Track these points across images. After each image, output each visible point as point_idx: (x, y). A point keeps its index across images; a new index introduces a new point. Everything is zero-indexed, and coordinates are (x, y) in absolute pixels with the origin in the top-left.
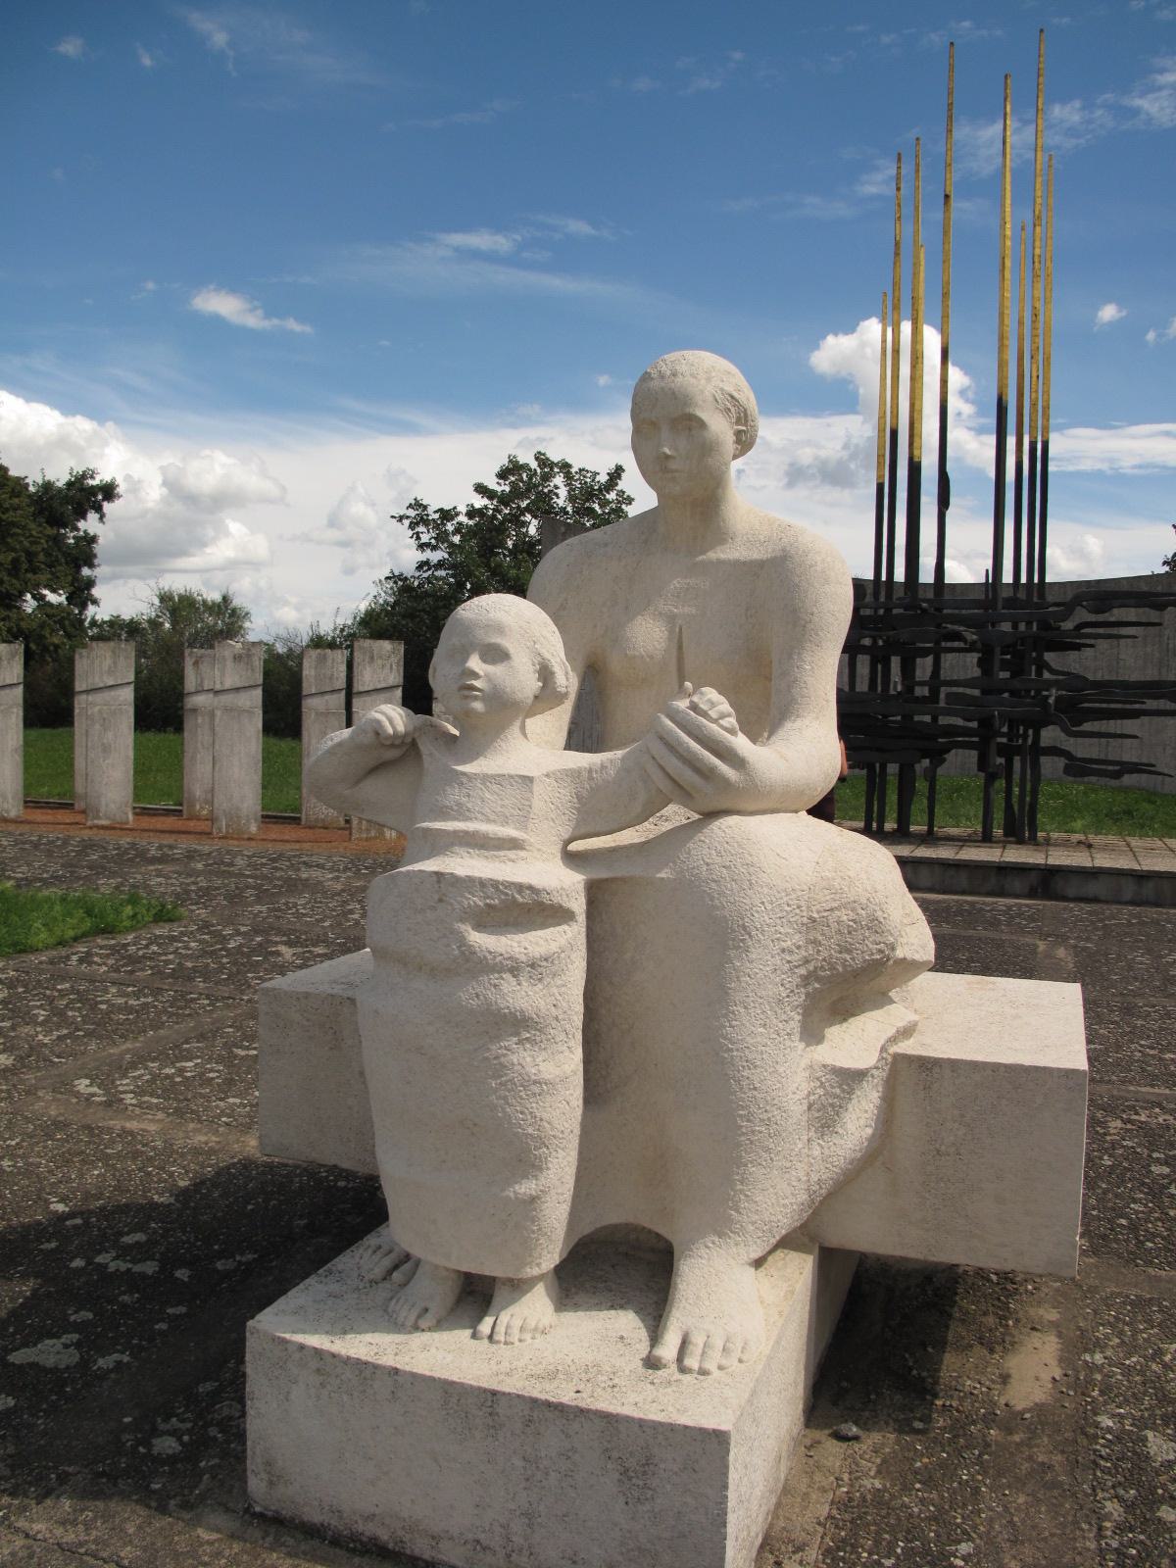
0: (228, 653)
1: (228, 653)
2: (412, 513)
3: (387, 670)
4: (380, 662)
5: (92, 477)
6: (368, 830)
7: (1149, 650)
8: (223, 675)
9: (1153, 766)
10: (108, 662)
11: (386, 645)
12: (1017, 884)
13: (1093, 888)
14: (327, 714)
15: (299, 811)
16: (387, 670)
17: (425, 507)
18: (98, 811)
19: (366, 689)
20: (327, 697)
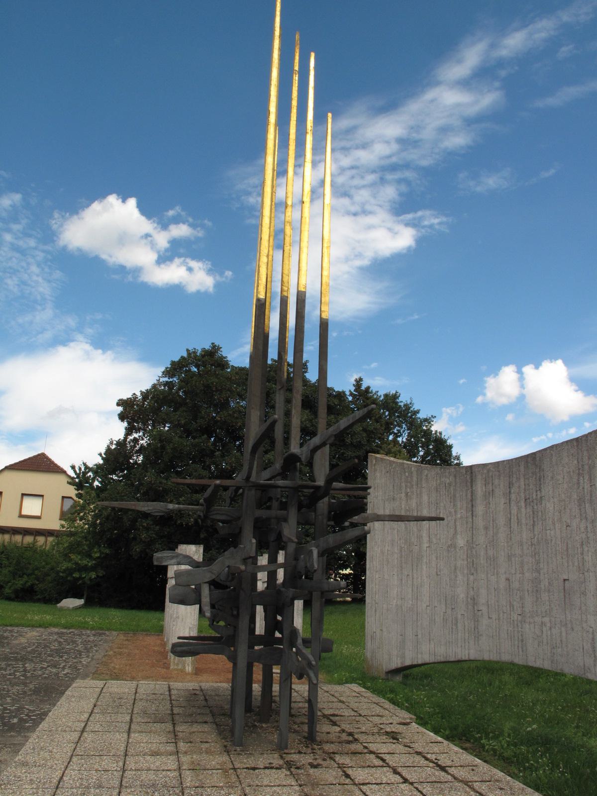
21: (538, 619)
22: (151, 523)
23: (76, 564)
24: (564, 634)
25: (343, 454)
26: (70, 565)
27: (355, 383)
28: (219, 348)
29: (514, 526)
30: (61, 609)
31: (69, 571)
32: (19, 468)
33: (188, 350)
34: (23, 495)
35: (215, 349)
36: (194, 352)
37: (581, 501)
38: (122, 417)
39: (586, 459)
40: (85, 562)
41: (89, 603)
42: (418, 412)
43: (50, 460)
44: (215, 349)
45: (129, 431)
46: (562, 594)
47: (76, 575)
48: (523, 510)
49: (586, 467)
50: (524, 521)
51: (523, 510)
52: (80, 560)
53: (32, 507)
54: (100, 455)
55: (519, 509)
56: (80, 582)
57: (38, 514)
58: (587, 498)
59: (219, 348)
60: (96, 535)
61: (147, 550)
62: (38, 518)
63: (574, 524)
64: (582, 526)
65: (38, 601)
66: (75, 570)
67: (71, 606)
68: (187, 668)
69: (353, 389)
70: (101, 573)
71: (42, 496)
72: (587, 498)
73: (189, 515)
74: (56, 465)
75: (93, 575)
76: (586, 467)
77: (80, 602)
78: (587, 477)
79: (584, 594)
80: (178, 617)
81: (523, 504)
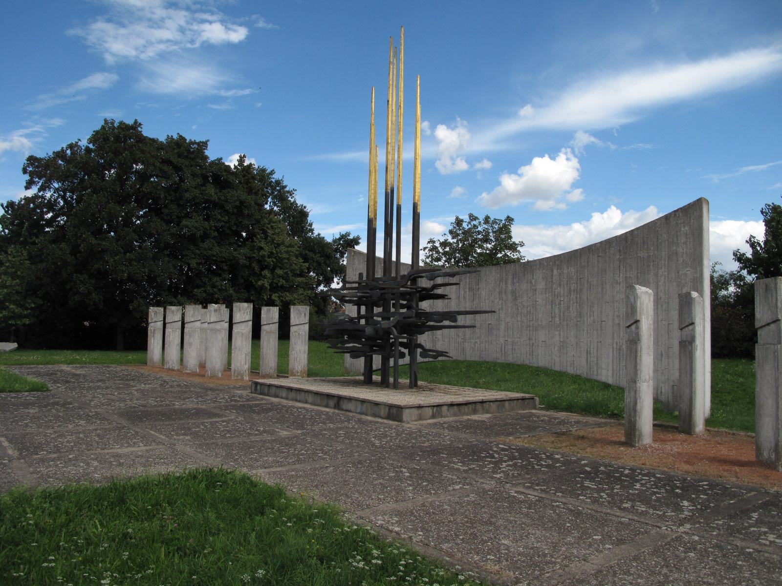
0: (212, 309)
1: (212, 309)
2: (429, 245)
3: (245, 314)
4: (243, 311)
5: (349, 236)
6: (237, 376)
7: (547, 295)
8: (210, 316)
9: (447, 353)
10: (192, 312)
11: (246, 305)
12: (332, 403)
13: (351, 406)
14: (271, 332)
15: (258, 369)
16: (245, 314)
17: (434, 242)
18: (187, 367)
19: (238, 321)
20: (271, 325)
21: (473, 341)
23: (13, 312)
24: (487, 346)
25: (241, 222)
27: (239, 158)
29: (462, 299)
35: (137, 124)
36: (113, 123)
37: (500, 293)
39: (504, 275)
40: (18, 310)
41: (22, 347)
42: (285, 187)
44: (137, 124)
46: (487, 330)
48: (468, 293)
49: (504, 279)
50: (468, 297)
51: (468, 293)
55: (465, 292)
58: (504, 291)
63: (496, 301)
64: (500, 303)
66: (11, 318)
67: (8, 349)
68: (245, 378)
69: (237, 164)
72: (504, 291)
75: (27, 321)
76: (504, 279)
78: (504, 283)
79: (499, 329)
80: (236, 348)
81: (467, 290)
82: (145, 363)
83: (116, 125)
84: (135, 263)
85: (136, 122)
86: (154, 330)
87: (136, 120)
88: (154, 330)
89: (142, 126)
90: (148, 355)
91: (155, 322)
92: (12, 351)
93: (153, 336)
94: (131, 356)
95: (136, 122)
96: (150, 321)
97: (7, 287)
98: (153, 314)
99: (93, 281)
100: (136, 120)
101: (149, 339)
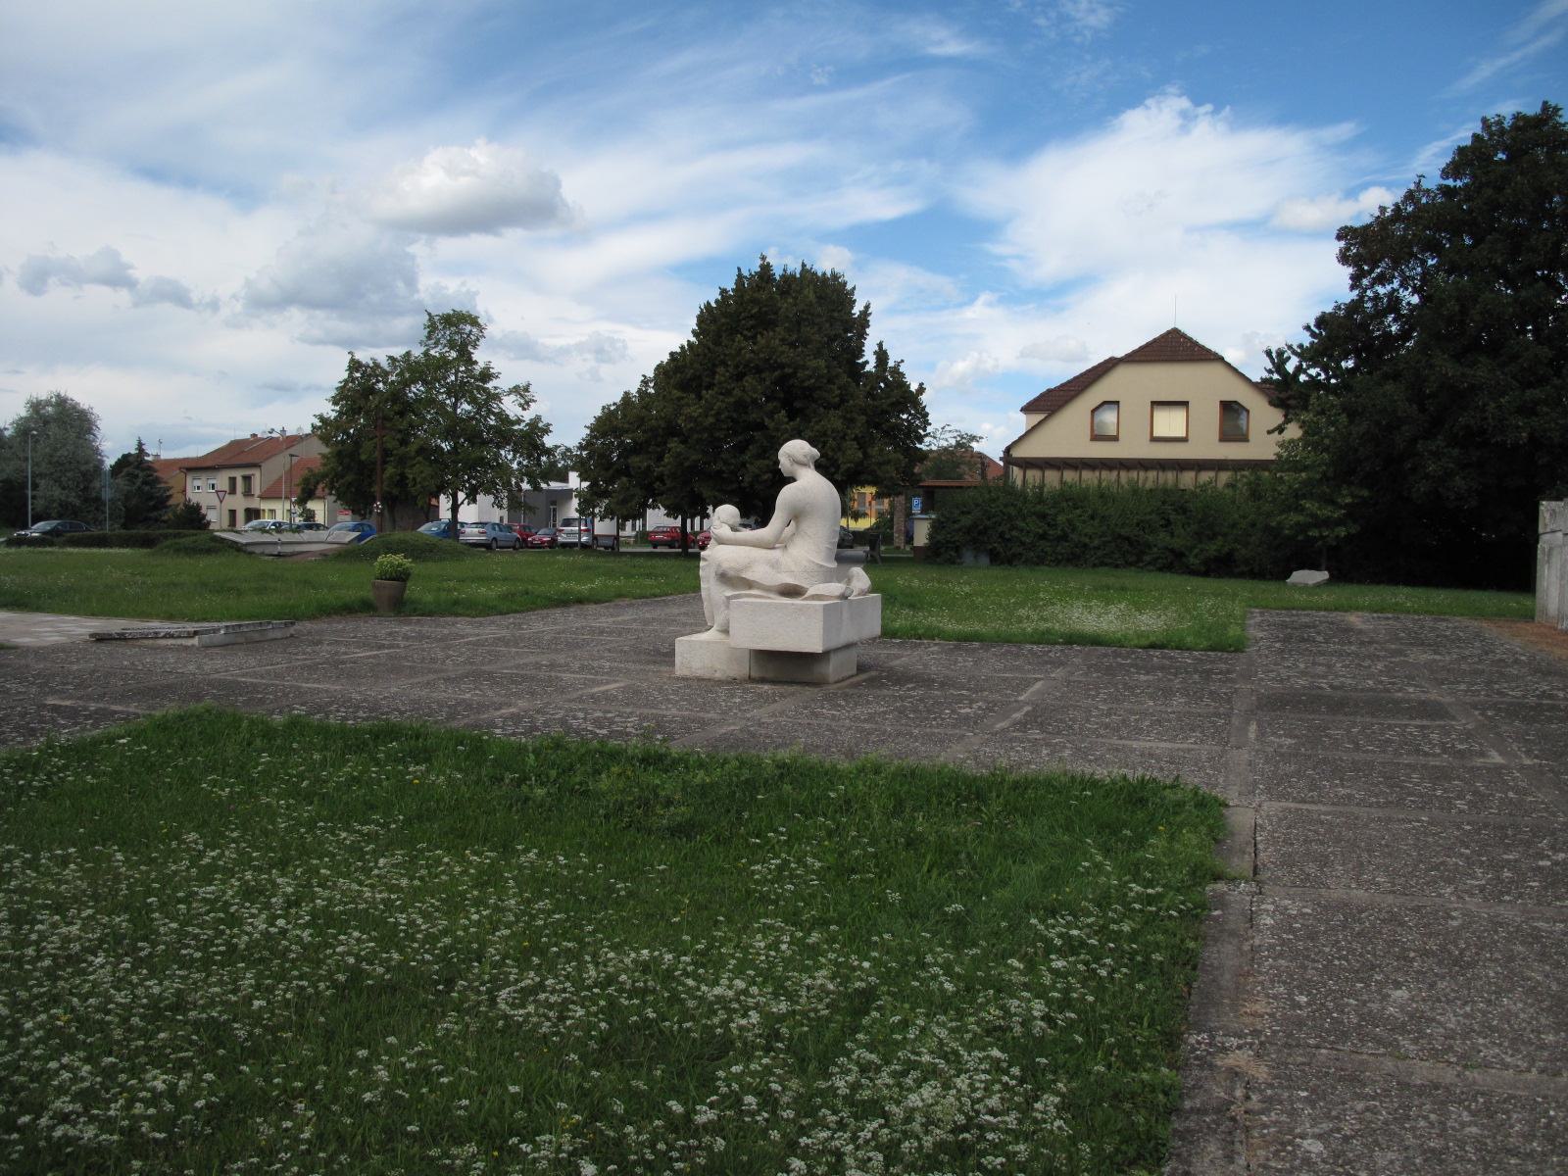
22: (1443, 444)
23: (1313, 516)
26: (1301, 518)
28: (1557, 110)
30: (1294, 585)
31: (1302, 528)
32: (1143, 358)
33: (1484, 121)
34: (1155, 404)
36: (1499, 123)
38: (1344, 258)
40: (1326, 512)
41: (1339, 577)
43: (1190, 339)
45: (1356, 280)
47: (1314, 533)
52: (1320, 509)
53: (1170, 423)
54: (1308, 328)
56: (1320, 543)
57: (1182, 433)
59: (1557, 110)
60: (1344, 468)
61: (1440, 489)
62: (1184, 440)
65: (1241, 575)
70: (1354, 529)
71: (1185, 404)
73: (1518, 427)
74: (1202, 348)
75: (1342, 532)
77: (1324, 575)
82: (1529, 616)
83: (1507, 124)
84: (1545, 409)
85: (1545, 106)
86: (1551, 549)
87: (1545, 103)
88: (1551, 549)
89: (1560, 113)
90: (1537, 601)
91: (1553, 532)
92: (1318, 585)
93: (1548, 562)
94: (1511, 601)
95: (1545, 106)
96: (1541, 530)
97: (1306, 468)
98: (1547, 515)
99: (1456, 452)
100: (1545, 103)
101: (1538, 568)
